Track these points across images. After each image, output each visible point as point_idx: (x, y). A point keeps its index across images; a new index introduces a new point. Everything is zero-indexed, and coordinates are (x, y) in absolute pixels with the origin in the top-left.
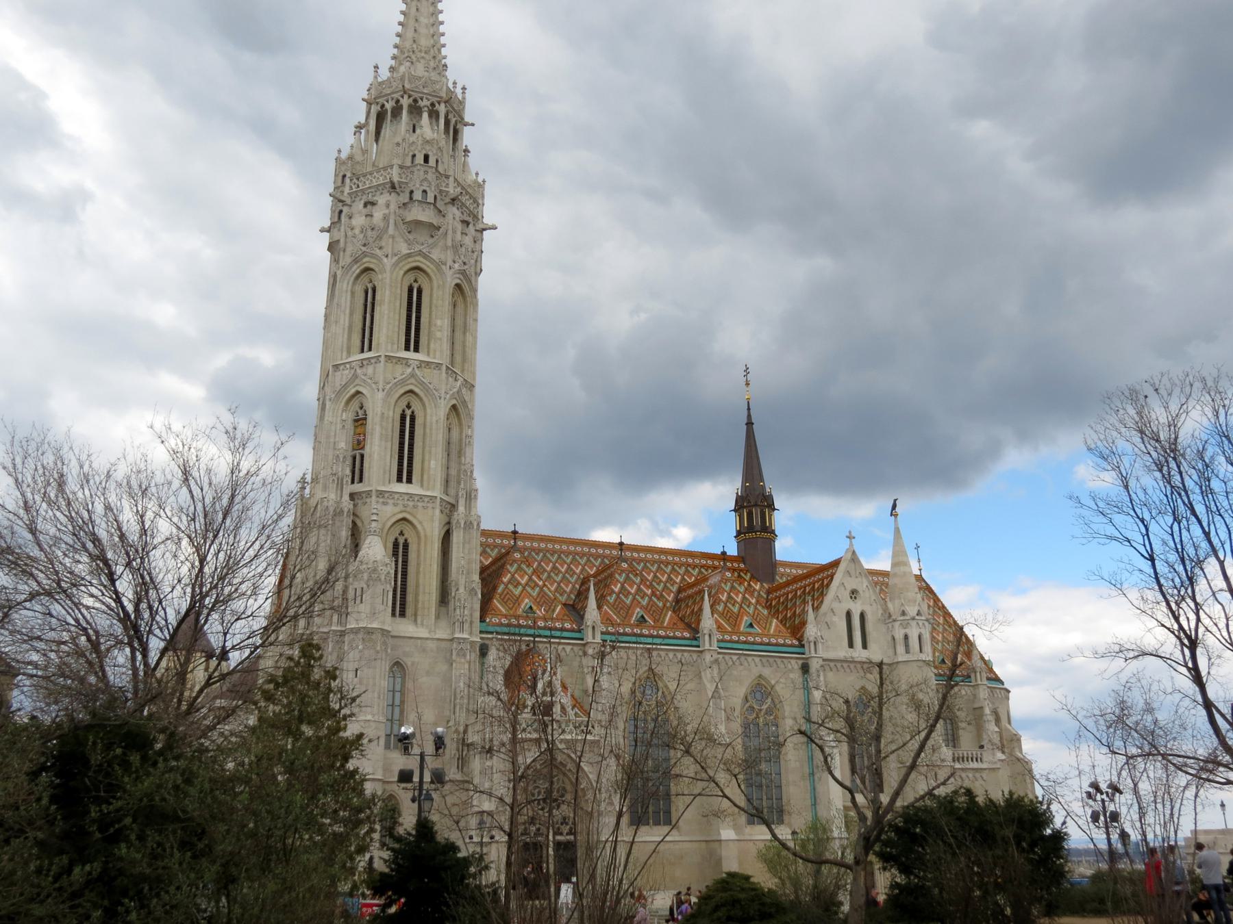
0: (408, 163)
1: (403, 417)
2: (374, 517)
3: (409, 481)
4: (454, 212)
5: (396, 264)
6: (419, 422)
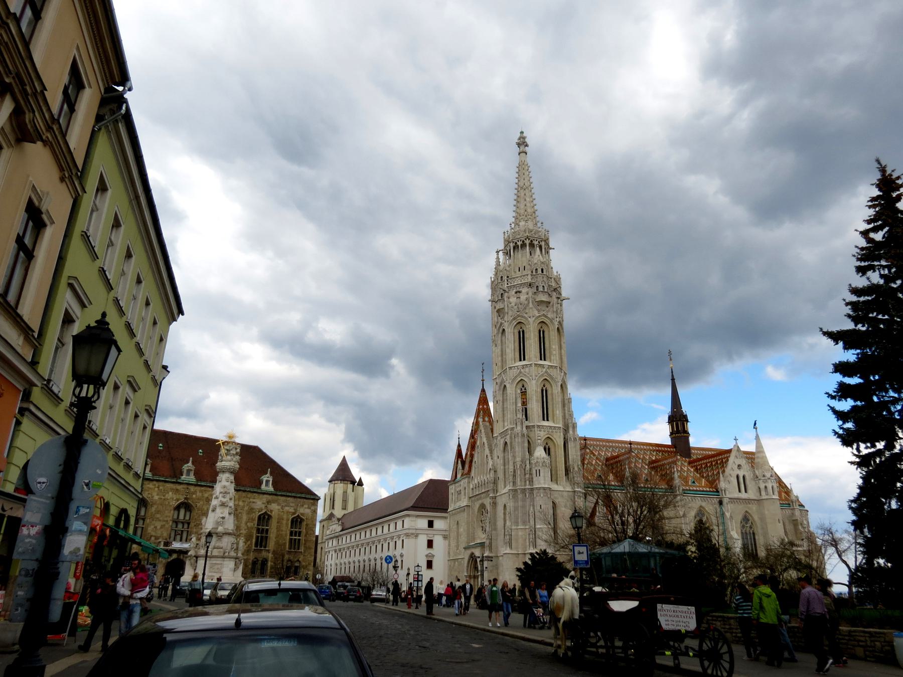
0: (534, 273)
1: (542, 391)
2: (539, 438)
3: (548, 420)
4: (554, 294)
5: (534, 321)
6: (549, 392)
